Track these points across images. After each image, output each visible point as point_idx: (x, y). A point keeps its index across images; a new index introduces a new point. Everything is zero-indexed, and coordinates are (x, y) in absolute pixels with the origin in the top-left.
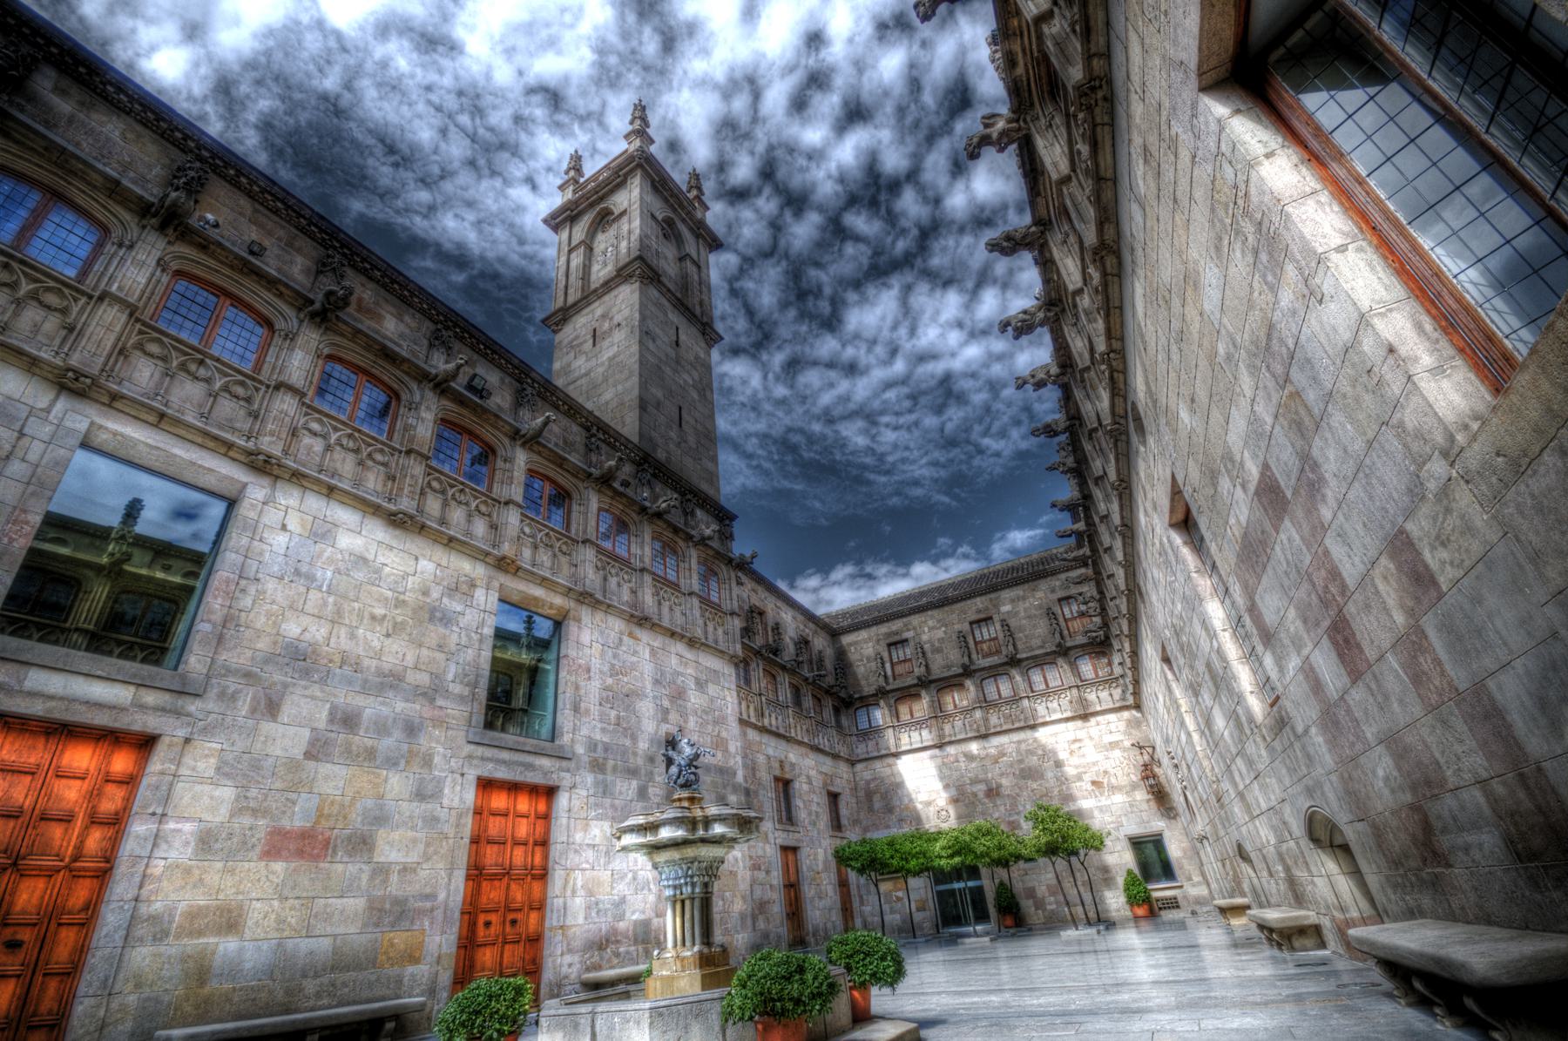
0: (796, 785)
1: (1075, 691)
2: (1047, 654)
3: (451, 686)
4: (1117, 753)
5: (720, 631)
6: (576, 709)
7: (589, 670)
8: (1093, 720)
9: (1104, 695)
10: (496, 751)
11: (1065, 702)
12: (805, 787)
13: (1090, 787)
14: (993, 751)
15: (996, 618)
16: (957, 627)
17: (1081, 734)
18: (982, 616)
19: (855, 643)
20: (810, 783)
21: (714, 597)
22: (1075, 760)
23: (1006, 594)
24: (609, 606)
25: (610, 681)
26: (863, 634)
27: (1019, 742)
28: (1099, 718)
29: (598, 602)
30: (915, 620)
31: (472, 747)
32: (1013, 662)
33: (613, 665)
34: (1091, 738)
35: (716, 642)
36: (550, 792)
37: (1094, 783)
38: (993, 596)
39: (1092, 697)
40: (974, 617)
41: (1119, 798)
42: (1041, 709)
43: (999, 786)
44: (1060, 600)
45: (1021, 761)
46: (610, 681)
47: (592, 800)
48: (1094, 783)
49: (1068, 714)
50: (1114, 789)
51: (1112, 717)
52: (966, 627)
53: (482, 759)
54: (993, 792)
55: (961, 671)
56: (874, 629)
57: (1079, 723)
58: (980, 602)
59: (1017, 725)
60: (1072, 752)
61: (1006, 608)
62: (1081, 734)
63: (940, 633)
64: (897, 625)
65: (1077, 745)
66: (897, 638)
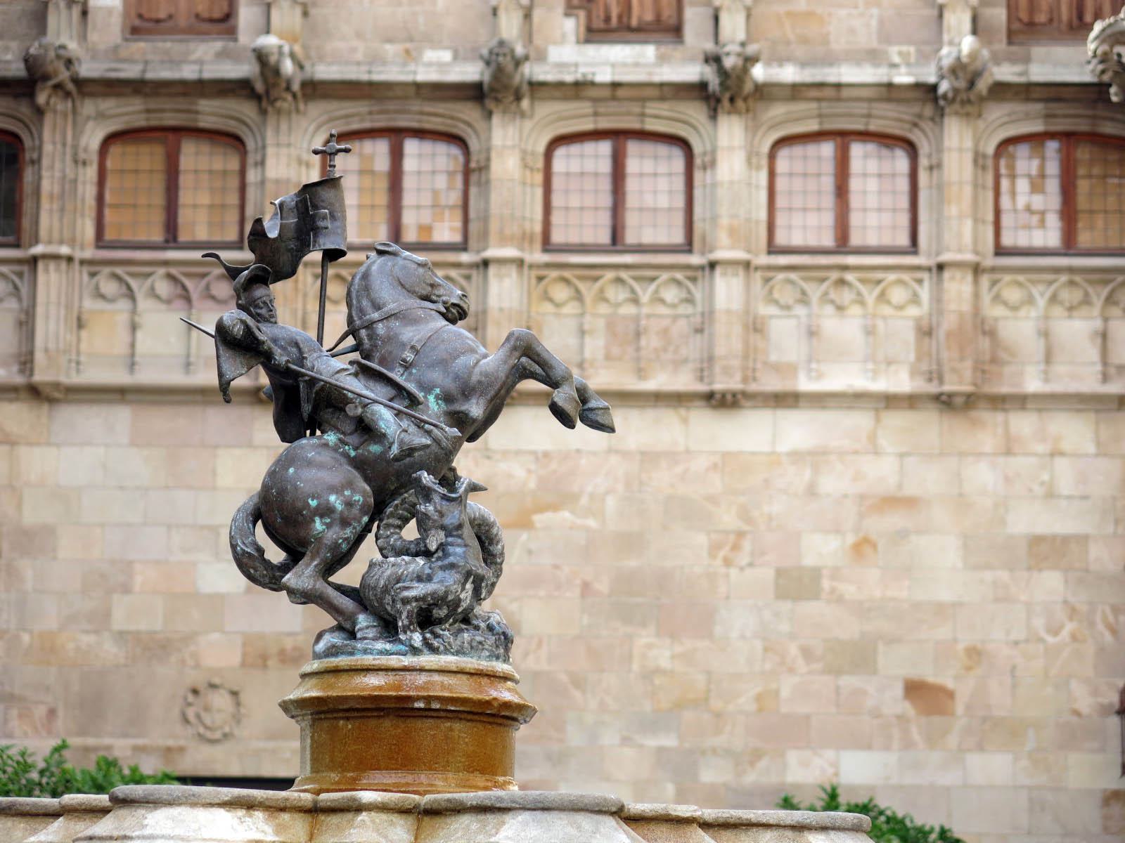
1: (958, 288)
2: (889, 91)
4: (1051, 583)
8: (989, 429)
9: (1077, 331)
11: (900, 327)
13: (894, 702)
17: (928, 479)
22: (868, 583)
27: (649, 458)
28: (1023, 423)
32: (725, 91)
34: (961, 502)
39: (1020, 328)
41: (994, 767)
42: (785, 335)
45: (630, 542)
48: (915, 689)
49: (902, 382)
50: (994, 730)
51: (1075, 431)
55: (471, 72)
57: (929, 424)
59: (650, 385)
60: (862, 547)
62: (928, 479)
65: (894, 520)
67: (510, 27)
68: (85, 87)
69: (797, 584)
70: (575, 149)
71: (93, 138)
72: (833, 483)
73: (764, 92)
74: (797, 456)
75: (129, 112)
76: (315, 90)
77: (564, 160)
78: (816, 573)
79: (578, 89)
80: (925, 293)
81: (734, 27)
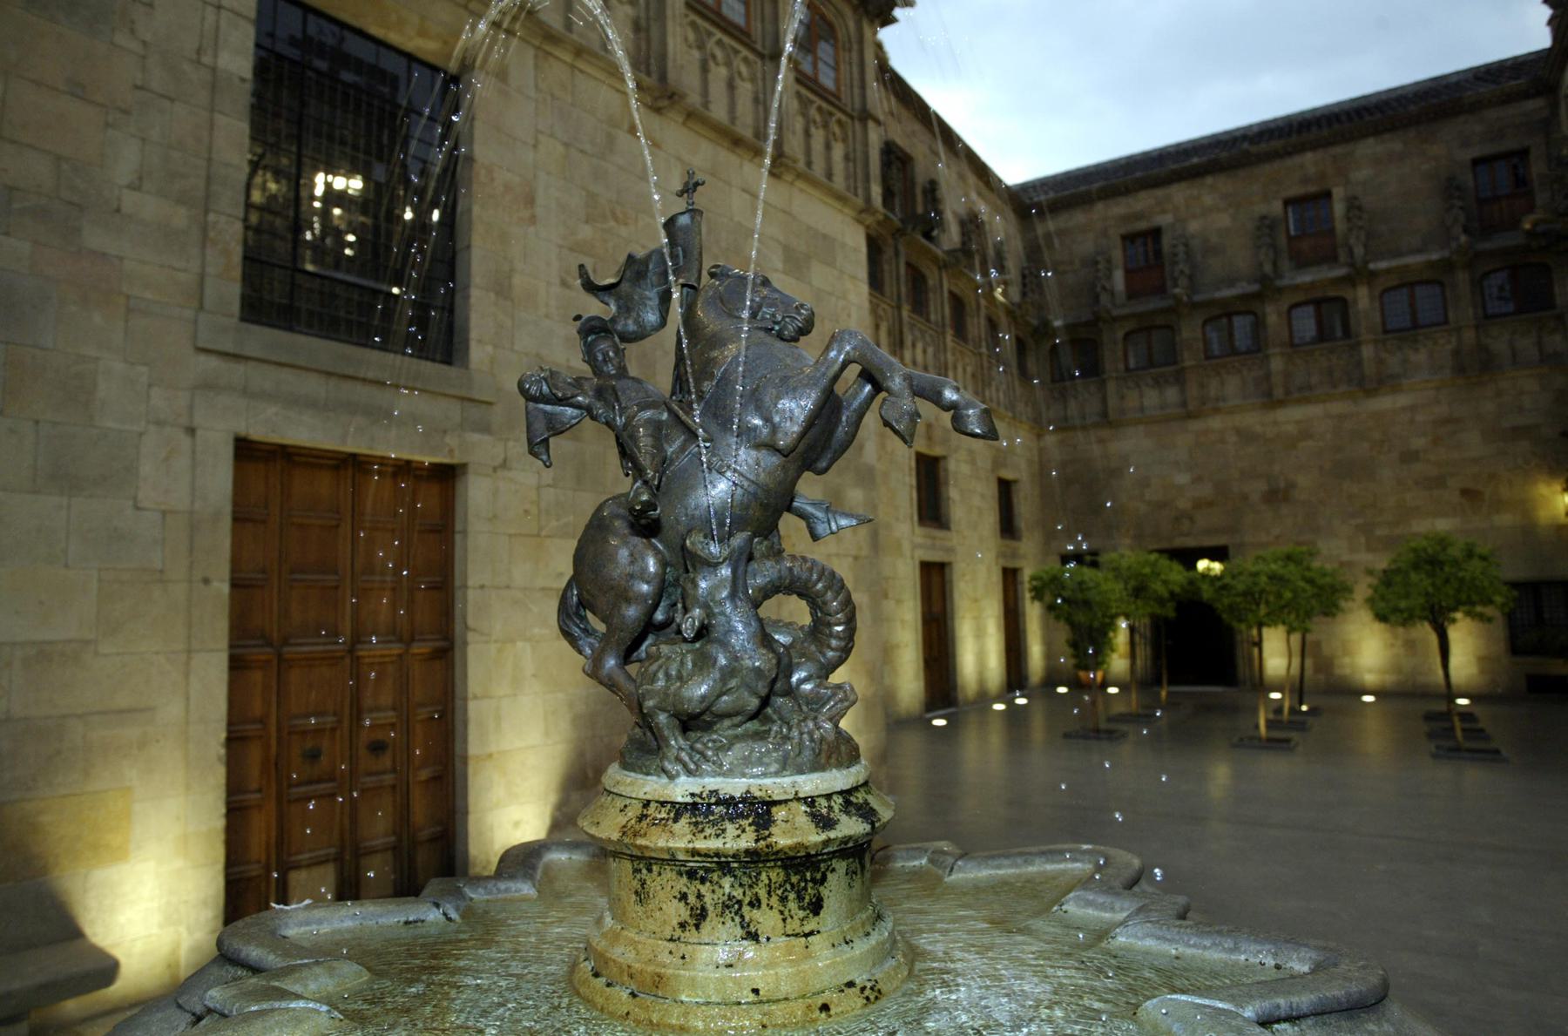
0: (952, 465)
3: (129, 200)
5: (838, 151)
6: (502, 289)
7: (530, 200)
10: (286, 375)
12: (965, 469)
14: (1291, 429)
15: (1338, 193)
16: (1260, 209)
18: (1312, 189)
19: (1061, 233)
20: (973, 462)
21: (827, 79)
23: (1368, 148)
24: (579, 52)
25: (586, 232)
26: (1078, 217)
29: (550, 37)
30: (1179, 193)
31: (213, 363)
33: (592, 197)
35: (829, 176)
36: (447, 476)
37: (1465, 492)
38: (1338, 150)
40: (1296, 190)
43: (1292, 486)
44: (1476, 162)
46: (586, 232)
47: (549, 495)
48: (1465, 492)
52: (1277, 207)
53: (245, 392)
54: (1277, 495)
55: (1255, 288)
56: (1100, 206)
58: (1309, 161)
61: (1361, 174)
63: (1223, 220)
64: (1143, 201)
66: (1142, 225)
67: (1268, 268)
68: (1115, 319)
69: (1409, 457)
70: (1299, 310)
71: (1120, 334)
72: (1420, 418)
73: (1373, 275)
74: (1404, 409)
75: (1130, 325)
76: (1195, 306)
77: (1297, 313)
78: (1417, 452)
79: (1296, 288)
80: (1454, 339)
81: (1359, 251)
